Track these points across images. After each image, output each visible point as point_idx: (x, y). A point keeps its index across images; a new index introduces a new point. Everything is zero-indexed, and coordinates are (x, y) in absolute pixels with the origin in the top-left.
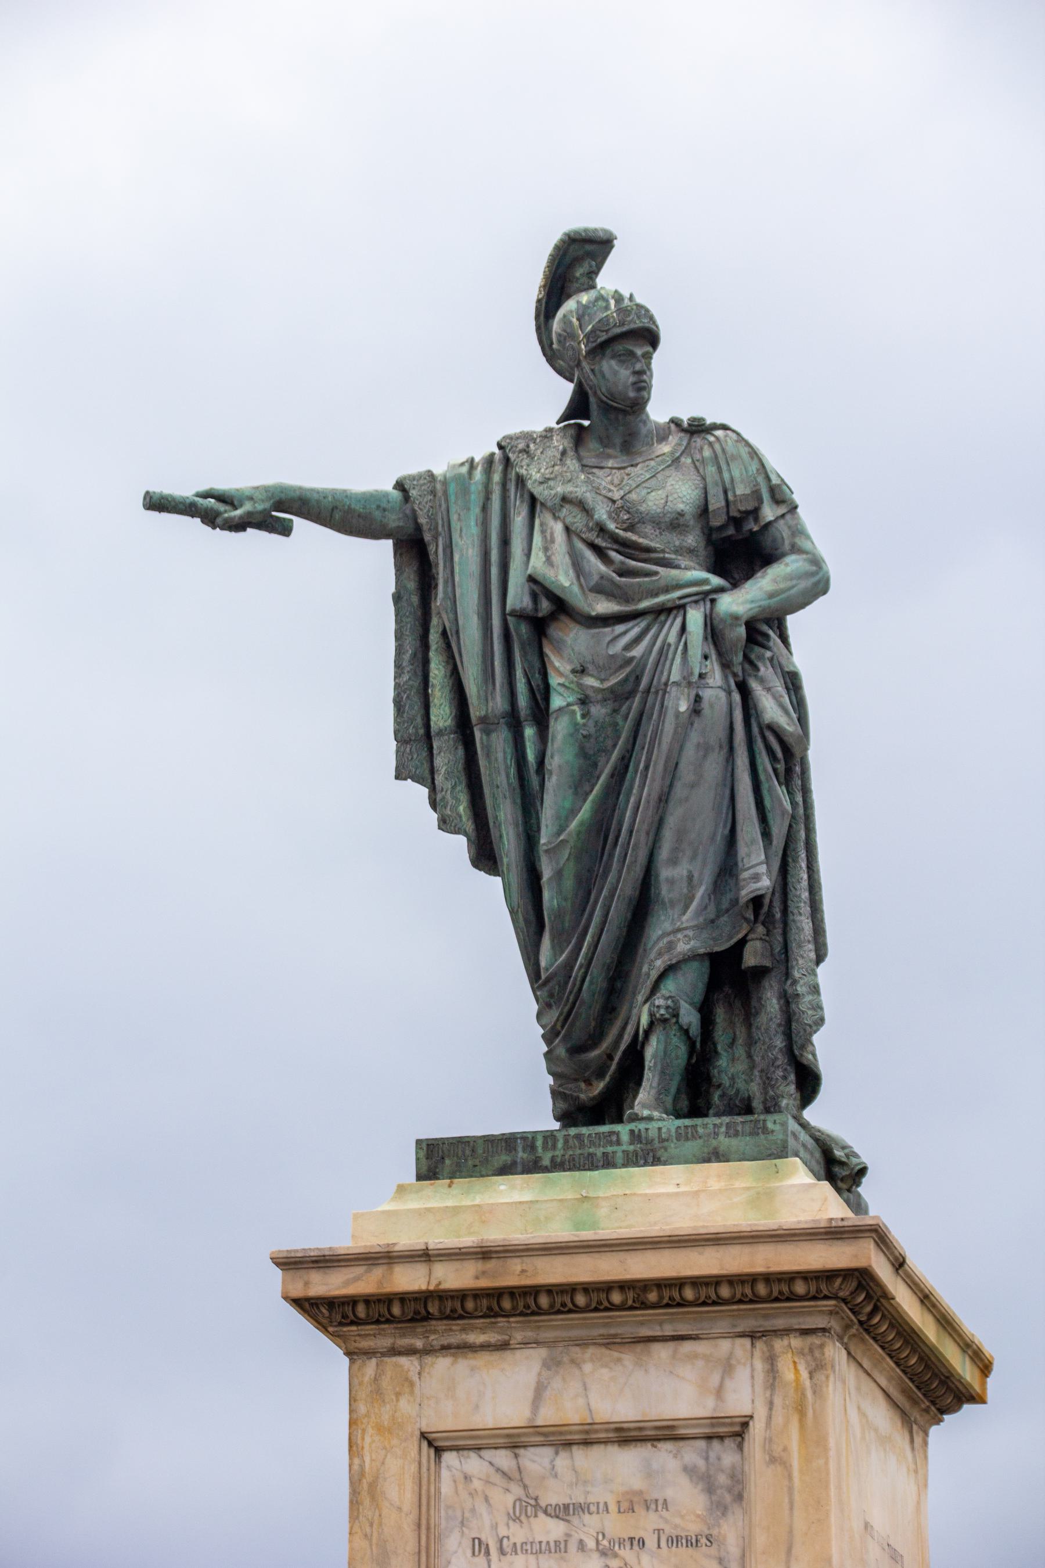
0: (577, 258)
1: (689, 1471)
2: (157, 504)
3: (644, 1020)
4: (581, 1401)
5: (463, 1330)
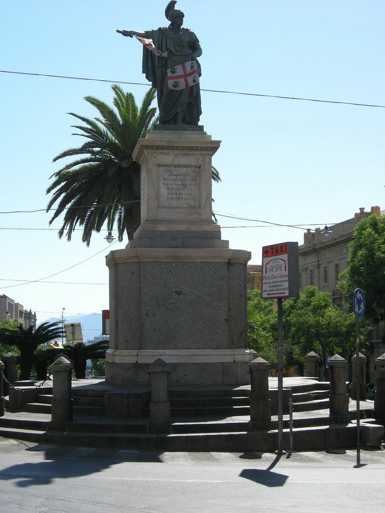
1: (193, 171)
2: (118, 31)
3: (180, 110)
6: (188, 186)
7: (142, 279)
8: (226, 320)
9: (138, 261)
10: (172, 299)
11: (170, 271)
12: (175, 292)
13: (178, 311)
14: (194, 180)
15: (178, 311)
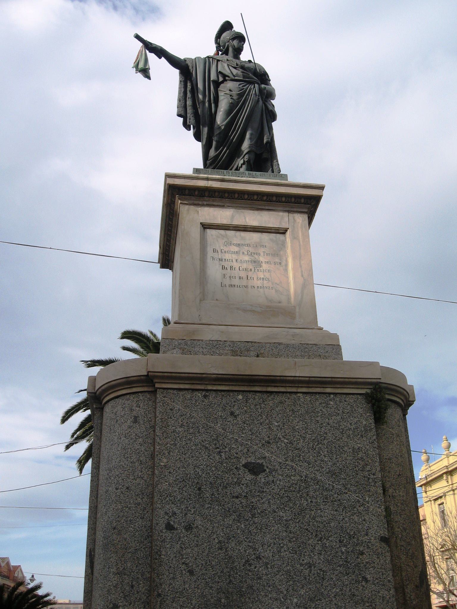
0: (227, 26)
1: (271, 240)
3: (242, 162)
4: (244, 220)
5: (213, 201)
7: (158, 432)
8: (384, 540)
9: (150, 389)
10: (238, 483)
11: (232, 414)
12: (246, 466)
13: (253, 516)
14: (275, 254)
15: (253, 516)
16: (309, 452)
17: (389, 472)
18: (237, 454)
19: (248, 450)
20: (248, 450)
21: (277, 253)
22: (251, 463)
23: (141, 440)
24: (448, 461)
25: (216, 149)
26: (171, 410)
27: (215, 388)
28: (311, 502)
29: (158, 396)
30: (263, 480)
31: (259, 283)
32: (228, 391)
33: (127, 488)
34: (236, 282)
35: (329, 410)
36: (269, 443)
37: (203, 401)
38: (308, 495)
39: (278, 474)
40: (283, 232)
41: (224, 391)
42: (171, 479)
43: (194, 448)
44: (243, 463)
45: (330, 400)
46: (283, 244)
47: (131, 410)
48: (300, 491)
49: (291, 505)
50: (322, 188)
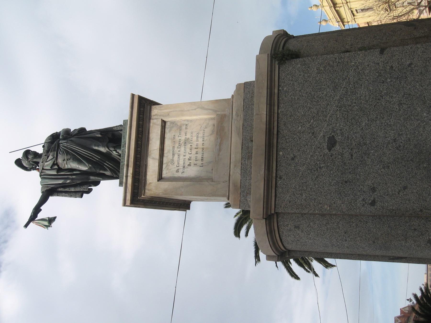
0: (18, 163)
1: (170, 131)
3: (114, 152)
6: (187, 137)
7: (306, 211)
8: (382, 51)
10: (342, 155)
11: (293, 159)
12: (330, 150)
13: (365, 144)
14: (180, 128)
15: (365, 144)
16: (320, 104)
17: (334, 48)
18: (321, 156)
19: (319, 148)
20: (319, 148)
21: (179, 128)
22: (328, 146)
23: (311, 224)
24: (326, 6)
25: (105, 170)
26: (290, 202)
27: (275, 171)
28: (355, 103)
29: (280, 211)
30: (340, 137)
31: (200, 140)
32: (277, 162)
33: (345, 233)
34: (199, 156)
35: (290, 91)
36: (313, 133)
37: (284, 179)
38: (350, 106)
39: (335, 126)
40: (164, 123)
41: (277, 165)
42: (339, 202)
43: (317, 186)
44: (328, 151)
45: (283, 89)
46: (173, 123)
47: (290, 230)
48: (347, 111)
49: (357, 117)
50: (133, 95)
